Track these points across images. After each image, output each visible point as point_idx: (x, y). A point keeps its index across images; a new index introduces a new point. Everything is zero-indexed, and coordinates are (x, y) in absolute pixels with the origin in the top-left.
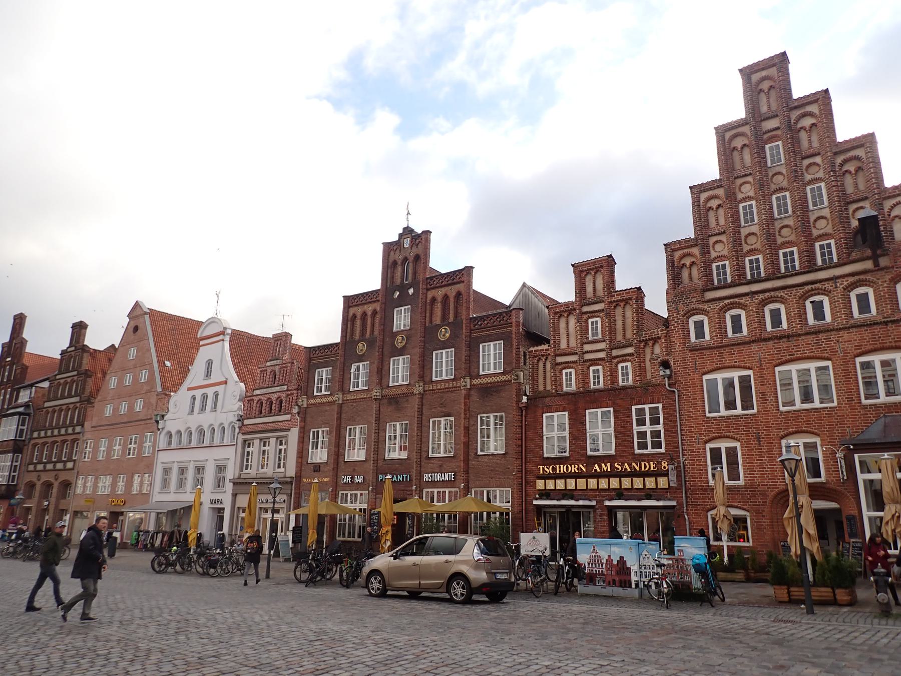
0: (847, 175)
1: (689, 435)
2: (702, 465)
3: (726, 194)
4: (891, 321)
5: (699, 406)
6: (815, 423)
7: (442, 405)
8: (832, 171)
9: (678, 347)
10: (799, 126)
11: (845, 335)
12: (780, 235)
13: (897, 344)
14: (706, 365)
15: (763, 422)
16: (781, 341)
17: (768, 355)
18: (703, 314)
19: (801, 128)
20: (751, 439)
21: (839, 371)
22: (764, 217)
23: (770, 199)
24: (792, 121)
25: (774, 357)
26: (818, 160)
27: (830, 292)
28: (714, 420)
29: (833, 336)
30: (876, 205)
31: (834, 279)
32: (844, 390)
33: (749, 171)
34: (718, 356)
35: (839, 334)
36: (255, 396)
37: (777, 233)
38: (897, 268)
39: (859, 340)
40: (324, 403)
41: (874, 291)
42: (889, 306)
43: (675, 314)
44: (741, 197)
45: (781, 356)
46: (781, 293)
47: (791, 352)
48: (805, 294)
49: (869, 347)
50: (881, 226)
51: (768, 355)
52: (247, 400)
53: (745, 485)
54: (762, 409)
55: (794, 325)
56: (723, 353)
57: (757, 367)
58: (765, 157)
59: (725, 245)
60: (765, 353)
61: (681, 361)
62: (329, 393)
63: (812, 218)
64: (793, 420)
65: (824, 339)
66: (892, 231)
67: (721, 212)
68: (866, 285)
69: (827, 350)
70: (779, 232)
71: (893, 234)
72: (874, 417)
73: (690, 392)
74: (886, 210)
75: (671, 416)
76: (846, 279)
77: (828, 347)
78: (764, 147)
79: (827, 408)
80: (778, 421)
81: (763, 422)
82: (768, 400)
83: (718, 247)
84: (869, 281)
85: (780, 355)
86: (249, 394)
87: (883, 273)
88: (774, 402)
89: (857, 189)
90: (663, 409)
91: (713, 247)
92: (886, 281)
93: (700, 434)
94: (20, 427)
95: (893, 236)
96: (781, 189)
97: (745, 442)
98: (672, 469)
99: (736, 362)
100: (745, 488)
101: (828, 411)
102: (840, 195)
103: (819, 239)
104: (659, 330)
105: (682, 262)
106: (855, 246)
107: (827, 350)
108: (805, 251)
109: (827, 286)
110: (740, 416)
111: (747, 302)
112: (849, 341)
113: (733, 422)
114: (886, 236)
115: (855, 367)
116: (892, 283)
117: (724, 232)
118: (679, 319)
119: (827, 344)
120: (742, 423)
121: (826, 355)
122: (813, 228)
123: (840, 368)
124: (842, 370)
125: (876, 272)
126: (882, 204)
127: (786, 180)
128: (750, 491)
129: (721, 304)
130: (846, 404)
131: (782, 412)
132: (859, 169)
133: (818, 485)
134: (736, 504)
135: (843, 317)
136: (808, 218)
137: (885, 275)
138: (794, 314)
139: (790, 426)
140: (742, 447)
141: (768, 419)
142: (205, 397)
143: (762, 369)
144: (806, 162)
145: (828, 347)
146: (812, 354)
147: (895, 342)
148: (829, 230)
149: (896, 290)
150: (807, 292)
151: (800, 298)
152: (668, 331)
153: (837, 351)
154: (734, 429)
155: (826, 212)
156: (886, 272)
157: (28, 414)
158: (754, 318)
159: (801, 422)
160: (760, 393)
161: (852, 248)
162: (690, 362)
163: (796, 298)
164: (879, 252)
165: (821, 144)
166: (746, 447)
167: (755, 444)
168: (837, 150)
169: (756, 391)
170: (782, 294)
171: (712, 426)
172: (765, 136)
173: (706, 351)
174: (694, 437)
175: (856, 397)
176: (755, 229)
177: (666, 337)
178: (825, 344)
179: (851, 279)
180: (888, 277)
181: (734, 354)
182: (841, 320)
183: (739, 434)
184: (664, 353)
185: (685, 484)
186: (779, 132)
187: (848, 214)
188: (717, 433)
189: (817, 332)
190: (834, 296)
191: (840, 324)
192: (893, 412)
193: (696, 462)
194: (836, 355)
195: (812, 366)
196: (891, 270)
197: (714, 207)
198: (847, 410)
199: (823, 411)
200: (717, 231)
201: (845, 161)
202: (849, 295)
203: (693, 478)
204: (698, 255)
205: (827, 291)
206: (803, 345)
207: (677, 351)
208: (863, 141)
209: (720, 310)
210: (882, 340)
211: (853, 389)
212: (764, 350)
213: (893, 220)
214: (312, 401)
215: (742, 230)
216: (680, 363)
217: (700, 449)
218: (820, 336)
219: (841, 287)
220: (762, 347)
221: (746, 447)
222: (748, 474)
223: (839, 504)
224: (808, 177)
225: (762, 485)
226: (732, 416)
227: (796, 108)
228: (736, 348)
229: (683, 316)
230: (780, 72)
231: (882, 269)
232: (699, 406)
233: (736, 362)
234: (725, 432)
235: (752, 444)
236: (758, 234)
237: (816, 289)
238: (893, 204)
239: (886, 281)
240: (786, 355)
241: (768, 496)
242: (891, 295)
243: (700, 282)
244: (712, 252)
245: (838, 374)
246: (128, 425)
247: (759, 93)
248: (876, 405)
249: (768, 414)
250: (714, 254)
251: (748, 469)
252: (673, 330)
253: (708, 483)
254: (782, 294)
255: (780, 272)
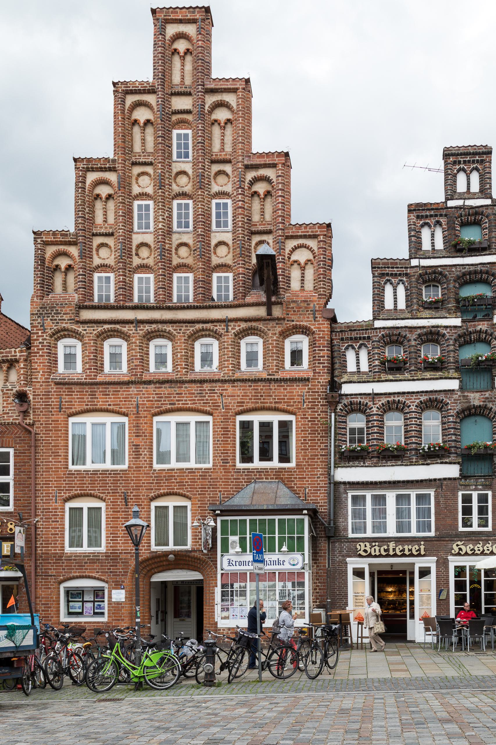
0: (256, 198)
1: (45, 490)
2: (58, 528)
3: (119, 183)
4: (274, 380)
5: (60, 456)
6: (188, 485)
8: (240, 187)
9: (40, 377)
10: (214, 117)
11: (230, 389)
12: (176, 254)
13: (277, 405)
14: (74, 405)
15: (133, 480)
16: (163, 386)
17: (147, 401)
18: (76, 338)
19: (216, 121)
20: (118, 499)
21: (218, 428)
22: (160, 226)
23: (170, 203)
24: (207, 108)
25: (154, 404)
26: (228, 168)
27: (221, 336)
28: (77, 474)
29: (217, 387)
30: (278, 243)
31: (226, 321)
32: (220, 450)
33: (150, 159)
34: (89, 395)
35: (224, 387)
37: (174, 251)
38: (288, 321)
39: (242, 396)
41: (264, 342)
42: (275, 362)
43: (40, 332)
44: (138, 193)
45: (162, 404)
46: (169, 328)
47: (172, 400)
48: (195, 333)
49: (250, 406)
50: (280, 268)
51: (147, 401)
53: (106, 553)
54: (134, 464)
55: (179, 369)
56: (95, 392)
57: (133, 414)
58: (170, 146)
59: (111, 251)
60: (145, 398)
61: (43, 395)
63: (214, 242)
64: (166, 480)
65: (209, 390)
66: (290, 277)
67: (111, 204)
68: (257, 335)
69: (209, 403)
70: (176, 249)
71: (290, 281)
72: (245, 482)
73: (51, 437)
74: (287, 251)
75: (25, 466)
76: (239, 323)
77: (211, 400)
78: (171, 131)
79: (201, 469)
80: (150, 480)
81: (133, 480)
82: (141, 455)
83: (104, 252)
84: (260, 331)
85: (160, 403)
87: (274, 323)
88: (147, 458)
89: (264, 218)
90: (15, 456)
91: (97, 250)
92: (276, 334)
93: (59, 490)
95: (290, 284)
96: (184, 195)
97: (111, 502)
98: (20, 532)
99: (110, 405)
100: (106, 556)
101: (202, 472)
102: (246, 221)
103: (217, 269)
104: (17, 350)
105: (56, 262)
106: (253, 287)
107: (209, 403)
108: (202, 281)
109: (220, 328)
110: (108, 471)
111: (131, 332)
112: (232, 396)
113: (99, 477)
114: (284, 282)
115: (235, 425)
116: (282, 337)
117: (112, 235)
118: (46, 339)
119: (211, 396)
120: (110, 480)
121: (208, 409)
122: (212, 254)
123: (220, 425)
124: (222, 428)
125: (267, 322)
126: (283, 243)
127: (191, 184)
128: (111, 559)
129: (100, 329)
130: (220, 466)
131: (155, 470)
132: (268, 194)
133: (184, 553)
134: (94, 575)
135: (230, 368)
136: (210, 241)
137: (275, 327)
138: (181, 356)
139: (162, 486)
140: (107, 508)
141: (139, 477)
143: (138, 417)
144: (215, 168)
145: (211, 400)
146: (194, 406)
147: (276, 403)
148: (228, 260)
149: (284, 345)
150: (198, 331)
151: (189, 337)
152: (30, 353)
153: (219, 406)
154: (100, 487)
155: (228, 238)
156: (277, 324)
158: (136, 353)
159: (173, 482)
160: (133, 445)
161: (249, 289)
162: (55, 398)
163: (184, 336)
164: (273, 299)
165: (234, 150)
166: (111, 508)
167: (122, 505)
168: (249, 163)
169: (129, 443)
170: (171, 328)
171: (74, 481)
172: (174, 118)
173: (75, 386)
174: (52, 493)
175: (231, 460)
176: (149, 239)
177: (26, 360)
178: (209, 396)
179: (243, 325)
180: (278, 329)
181: (109, 395)
182: (228, 370)
183: (105, 493)
184: (22, 382)
185: (36, 550)
186: (189, 117)
187: (250, 246)
188: (80, 490)
189: (202, 382)
190: (224, 342)
191: (226, 376)
192: (263, 478)
193: (52, 525)
194: (217, 410)
195: (192, 419)
196: (282, 322)
197: (104, 196)
198: (221, 472)
199: (198, 472)
200: (103, 231)
201: (256, 180)
202: (239, 343)
203: (45, 544)
204: (77, 258)
205: (218, 334)
206: (185, 394)
207: (39, 382)
208: (277, 160)
209: (98, 337)
210: (264, 399)
211: (230, 450)
212: (143, 394)
213: (292, 265)
215: (134, 236)
216: (41, 399)
217: (58, 509)
218: (205, 385)
219: (233, 331)
220: (142, 391)
221: (111, 508)
222: (111, 540)
223: (202, 573)
224: (215, 188)
225: (125, 553)
226: (99, 471)
227: (213, 91)
228: (111, 388)
229: (51, 337)
230: (200, 34)
231: (273, 320)
232: (60, 456)
233: (110, 405)
234: (89, 490)
235: (119, 505)
236: (153, 246)
237: (206, 330)
238: (295, 246)
239: (276, 334)
240: (167, 404)
241: (130, 565)
242: (278, 350)
243: (76, 295)
244: (95, 256)
245: (217, 431)
247: (173, 54)
248: (249, 469)
249: (140, 471)
250: (97, 261)
251: (111, 534)
252: (35, 353)
253: (64, 550)
254: (171, 328)
255: (172, 301)
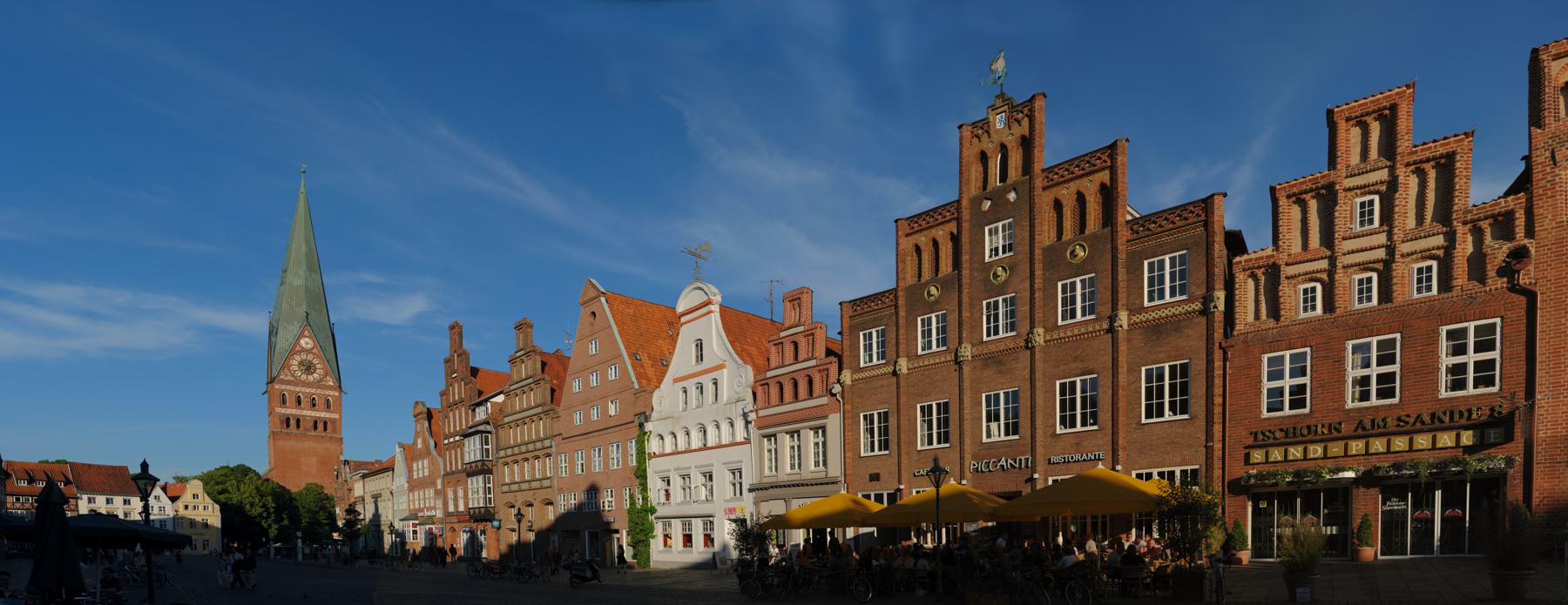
7: (1075, 359)
36: (769, 378)
40: (878, 375)
52: (761, 387)
62: (884, 361)
86: (761, 377)
94: (485, 447)
142: (701, 388)
157: (490, 433)
214: (856, 376)
246: (605, 431)
